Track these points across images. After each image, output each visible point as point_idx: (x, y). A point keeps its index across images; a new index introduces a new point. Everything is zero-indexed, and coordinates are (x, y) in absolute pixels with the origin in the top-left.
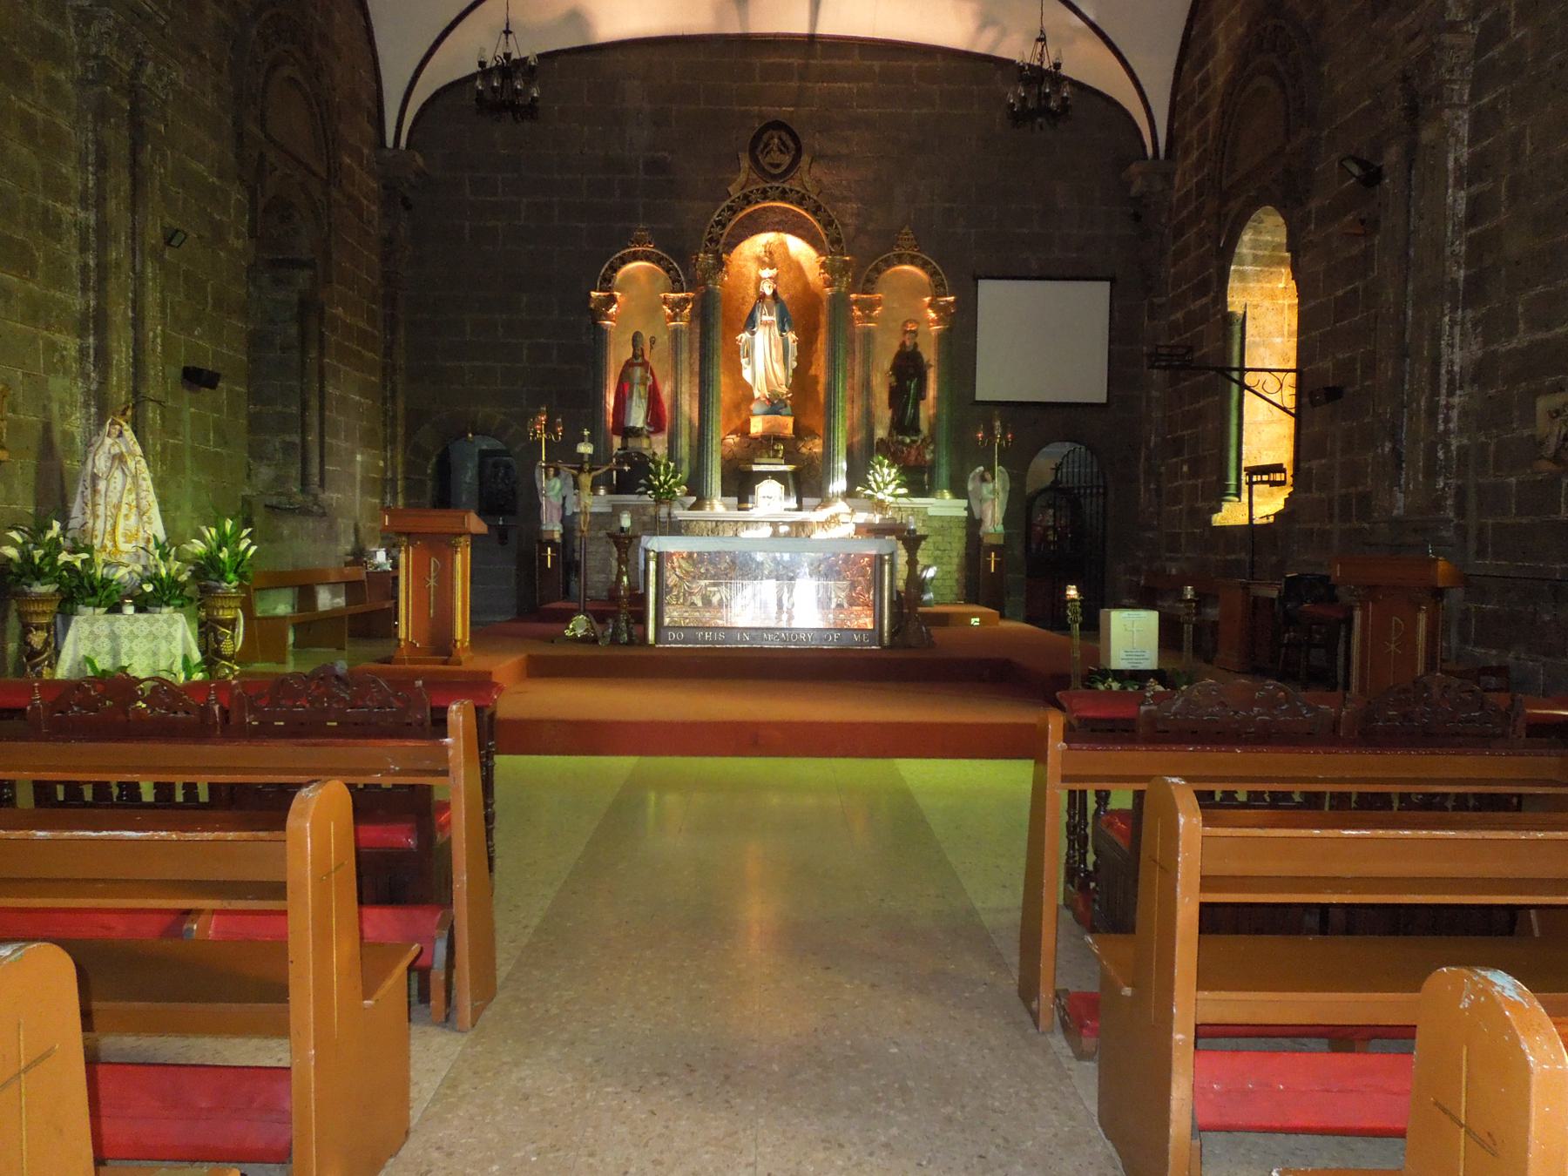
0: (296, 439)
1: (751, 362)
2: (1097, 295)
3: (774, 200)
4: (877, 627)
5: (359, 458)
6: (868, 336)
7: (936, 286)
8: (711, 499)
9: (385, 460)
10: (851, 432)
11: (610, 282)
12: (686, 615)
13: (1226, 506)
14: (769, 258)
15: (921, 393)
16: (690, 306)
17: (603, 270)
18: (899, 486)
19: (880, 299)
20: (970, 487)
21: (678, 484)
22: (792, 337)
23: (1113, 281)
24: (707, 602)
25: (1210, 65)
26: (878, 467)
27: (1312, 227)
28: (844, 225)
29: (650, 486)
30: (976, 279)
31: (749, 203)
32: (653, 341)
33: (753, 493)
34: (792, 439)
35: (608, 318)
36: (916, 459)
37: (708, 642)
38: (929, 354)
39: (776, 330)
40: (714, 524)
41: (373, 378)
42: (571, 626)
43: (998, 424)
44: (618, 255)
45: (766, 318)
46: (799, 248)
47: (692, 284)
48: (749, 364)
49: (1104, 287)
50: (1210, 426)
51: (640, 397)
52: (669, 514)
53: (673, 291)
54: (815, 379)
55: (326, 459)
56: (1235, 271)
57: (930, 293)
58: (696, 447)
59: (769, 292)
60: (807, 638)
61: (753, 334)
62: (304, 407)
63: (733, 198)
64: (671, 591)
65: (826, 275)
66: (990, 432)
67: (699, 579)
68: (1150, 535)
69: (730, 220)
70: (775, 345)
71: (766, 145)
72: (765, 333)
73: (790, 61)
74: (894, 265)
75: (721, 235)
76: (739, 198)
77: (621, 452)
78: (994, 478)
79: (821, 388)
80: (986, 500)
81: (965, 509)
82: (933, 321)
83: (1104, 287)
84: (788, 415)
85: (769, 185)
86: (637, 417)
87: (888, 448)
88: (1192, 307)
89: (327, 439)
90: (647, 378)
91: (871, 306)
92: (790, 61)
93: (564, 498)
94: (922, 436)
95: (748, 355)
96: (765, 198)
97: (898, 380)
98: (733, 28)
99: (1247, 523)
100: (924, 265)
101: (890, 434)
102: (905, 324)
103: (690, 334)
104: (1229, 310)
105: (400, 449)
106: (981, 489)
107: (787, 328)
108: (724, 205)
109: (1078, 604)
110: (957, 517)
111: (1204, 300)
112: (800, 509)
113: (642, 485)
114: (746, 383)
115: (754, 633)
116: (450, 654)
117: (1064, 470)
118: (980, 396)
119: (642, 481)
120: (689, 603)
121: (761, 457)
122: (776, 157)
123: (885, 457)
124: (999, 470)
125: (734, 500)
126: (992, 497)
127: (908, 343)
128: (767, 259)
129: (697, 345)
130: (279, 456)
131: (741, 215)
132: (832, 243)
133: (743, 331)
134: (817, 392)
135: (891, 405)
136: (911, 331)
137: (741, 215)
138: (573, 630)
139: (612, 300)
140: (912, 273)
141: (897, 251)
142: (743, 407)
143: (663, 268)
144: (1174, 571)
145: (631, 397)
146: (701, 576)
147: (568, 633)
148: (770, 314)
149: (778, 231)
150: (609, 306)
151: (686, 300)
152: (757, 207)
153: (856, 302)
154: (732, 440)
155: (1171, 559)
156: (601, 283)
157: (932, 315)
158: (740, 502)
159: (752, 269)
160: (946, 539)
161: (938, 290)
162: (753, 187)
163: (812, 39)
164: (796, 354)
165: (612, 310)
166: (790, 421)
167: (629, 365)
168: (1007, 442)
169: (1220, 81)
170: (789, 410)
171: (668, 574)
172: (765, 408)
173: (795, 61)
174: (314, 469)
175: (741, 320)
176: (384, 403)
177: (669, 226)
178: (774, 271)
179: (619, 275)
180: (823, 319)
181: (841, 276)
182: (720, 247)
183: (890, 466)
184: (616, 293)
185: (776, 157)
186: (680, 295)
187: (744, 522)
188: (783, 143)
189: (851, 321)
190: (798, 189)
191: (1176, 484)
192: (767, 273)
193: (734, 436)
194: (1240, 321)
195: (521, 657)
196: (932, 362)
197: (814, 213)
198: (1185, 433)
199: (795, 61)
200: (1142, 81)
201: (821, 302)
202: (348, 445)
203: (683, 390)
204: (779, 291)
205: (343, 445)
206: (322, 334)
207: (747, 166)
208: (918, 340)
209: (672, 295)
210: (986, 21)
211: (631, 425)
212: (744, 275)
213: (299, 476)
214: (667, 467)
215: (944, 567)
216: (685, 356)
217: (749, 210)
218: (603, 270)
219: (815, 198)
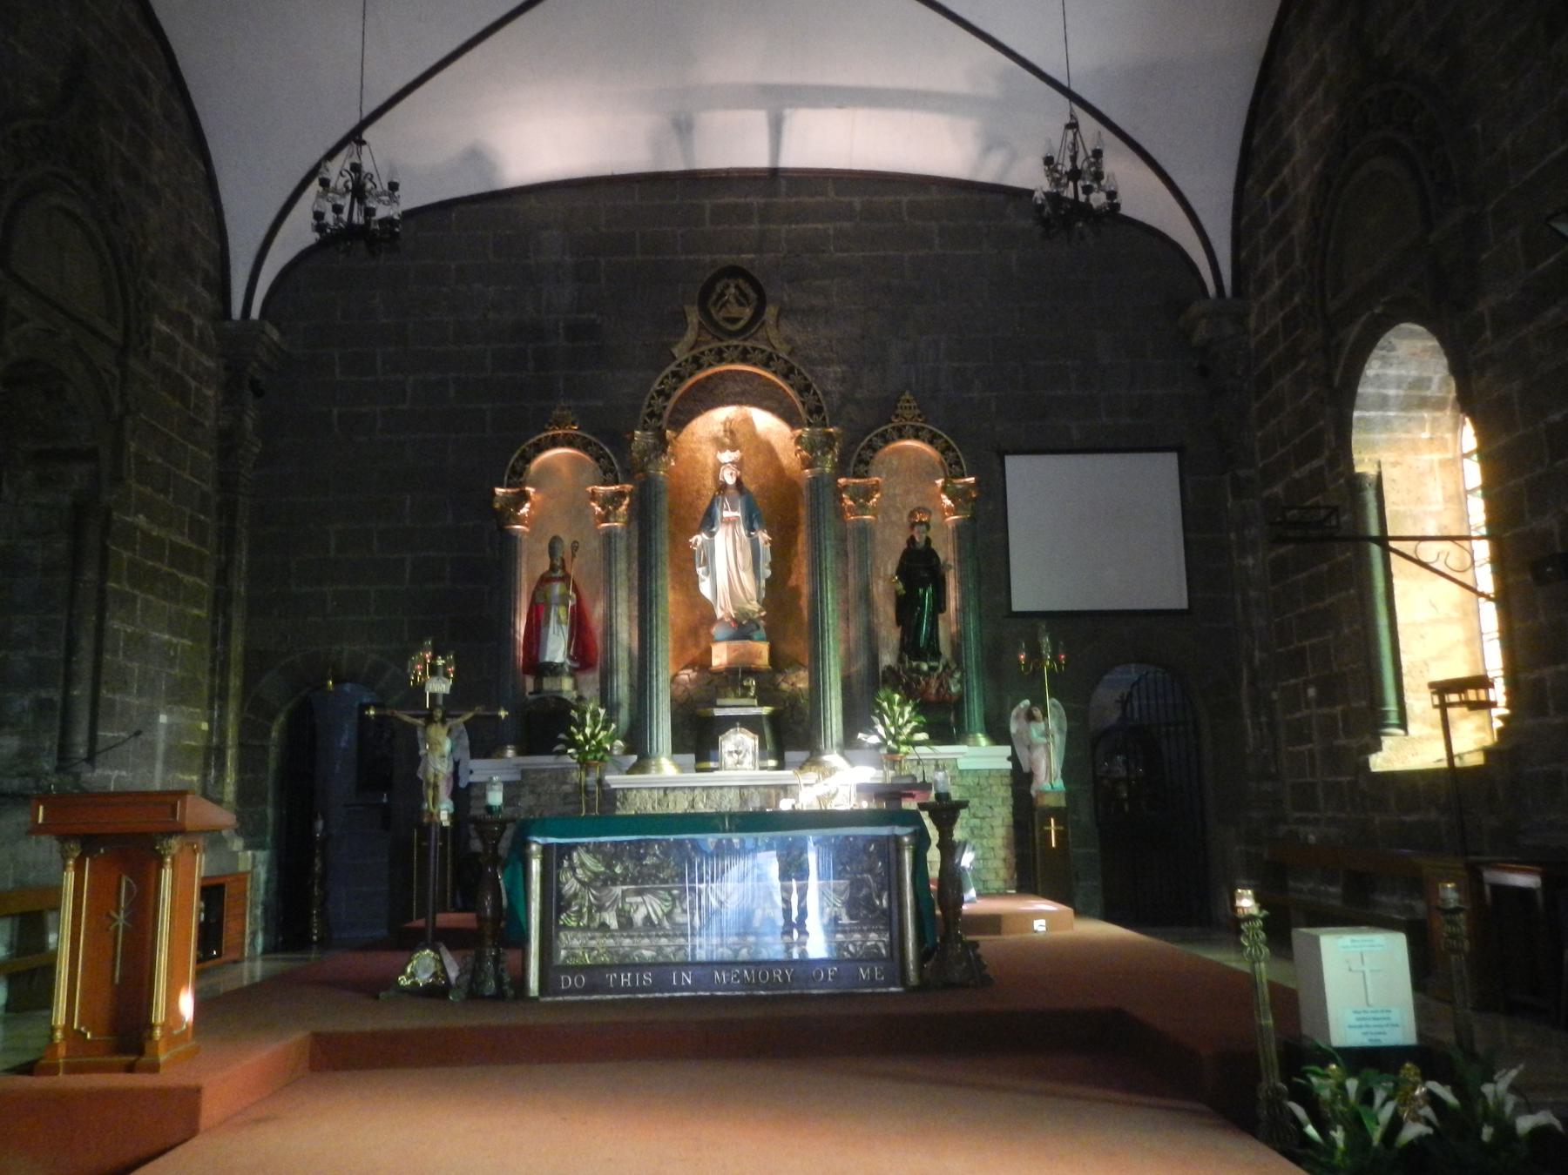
0: (56, 696)
1: (711, 573)
2: (1160, 471)
3: (732, 362)
4: (896, 954)
5: (163, 719)
6: (864, 531)
7: (950, 465)
8: (657, 757)
9: (210, 721)
10: (848, 659)
11: (521, 475)
12: (593, 943)
13: (1387, 742)
14: (732, 437)
15: (939, 604)
16: (627, 501)
17: (512, 461)
18: (916, 730)
20: (1013, 729)
21: (612, 739)
22: (763, 536)
23: (1180, 450)
24: (626, 923)
25: (1286, 171)
26: (885, 704)
27: (1488, 334)
28: (825, 393)
29: (572, 743)
30: (1001, 455)
31: (700, 367)
32: (575, 547)
33: (715, 745)
34: (769, 671)
35: (519, 521)
36: (938, 691)
37: (625, 990)
38: (946, 551)
40: (662, 793)
41: (196, 611)
42: (409, 970)
43: (1046, 640)
44: (531, 441)
45: (726, 514)
46: (766, 422)
47: (629, 476)
48: (707, 573)
49: (1171, 459)
50: (1346, 631)
51: (559, 622)
52: (600, 782)
53: (605, 483)
54: (796, 591)
55: (100, 722)
56: (1360, 419)
57: (942, 474)
58: (636, 685)
59: (731, 481)
60: (784, 974)
61: (712, 535)
62: (71, 648)
63: (677, 362)
64: (569, 906)
65: (804, 453)
66: (1035, 653)
67: (614, 884)
68: (1267, 786)
69: (675, 389)
70: (741, 549)
71: (722, 295)
72: (727, 534)
73: (748, 200)
74: (893, 440)
75: (665, 408)
76: (686, 361)
77: (534, 697)
78: (1045, 715)
79: (804, 602)
80: (1037, 746)
81: (1009, 759)
82: (949, 507)
83: (1171, 459)
84: (761, 640)
85: (725, 344)
86: (557, 649)
87: (899, 678)
88: (1296, 475)
89: (104, 693)
90: (570, 597)
91: (868, 497)
92: (748, 200)
93: (456, 764)
94: (942, 661)
95: (705, 562)
96: (721, 360)
97: (906, 587)
98: (675, 164)
99: (1444, 764)
101: (900, 660)
102: (912, 514)
103: (628, 539)
104: (1358, 469)
105: (233, 706)
106: (1028, 732)
107: (756, 525)
108: (667, 371)
109: (1259, 923)
110: (998, 770)
111: (1315, 463)
112: (781, 767)
113: (562, 741)
114: (706, 600)
115: (700, 971)
116: (140, 1051)
117: (1136, 703)
118: (1022, 601)
119: (562, 736)
120: (596, 924)
121: (726, 696)
122: (734, 310)
123: (895, 690)
124: (1054, 705)
125: (690, 758)
126: (1044, 740)
127: (917, 539)
128: (727, 441)
129: (635, 553)
130: (28, 719)
131: (690, 382)
132: (810, 413)
133: (698, 532)
134: (800, 609)
135: (900, 620)
136: (921, 523)
137: (690, 382)
138: (413, 975)
139: (524, 497)
140: (916, 450)
141: (896, 422)
142: (702, 632)
143: (591, 455)
144: (1312, 838)
145: (547, 623)
146: (613, 880)
147: (404, 981)
148: (734, 509)
149: (740, 403)
150: (519, 506)
151: (621, 495)
152: (710, 371)
153: (845, 487)
154: (687, 675)
155: (1303, 821)
156: (509, 478)
157: (947, 502)
158: (698, 760)
159: (708, 454)
160: (985, 802)
161: (953, 469)
162: (705, 348)
163: (774, 173)
164: (769, 558)
165: (524, 510)
166: (763, 648)
167: (545, 580)
168: (1059, 665)
169: (1302, 187)
170: (762, 632)
171: (563, 879)
172: (730, 632)
173: (756, 201)
174: (80, 737)
175: (695, 519)
176: (214, 642)
177: (600, 403)
178: (736, 455)
179: (534, 466)
180: (803, 512)
181: (824, 454)
182: (664, 423)
183: (902, 704)
184: (527, 488)
185: (734, 310)
186: (613, 488)
187: (704, 788)
188: (745, 296)
189: (840, 513)
190: (763, 347)
191: (1298, 715)
192: (727, 457)
193: (689, 671)
194: (1374, 484)
195: (297, 1037)
196: (951, 562)
197: (786, 377)
198: (1306, 643)
199: (756, 201)
200: (1195, 206)
201: (800, 491)
202: (144, 700)
203: (619, 611)
204: (745, 479)
205: (134, 701)
206: (105, 548)
207: (695, 320)
208: (931, 534)
209: (602, 488)
210: (991, 143)
211: (547, 659)
212: (697, 462)
213: (55, 748)
214: (595, 715)
215: (985, 842)
216: (621, 566)
217: (701, 375)
218: (512, 461)
219: (786, 357)
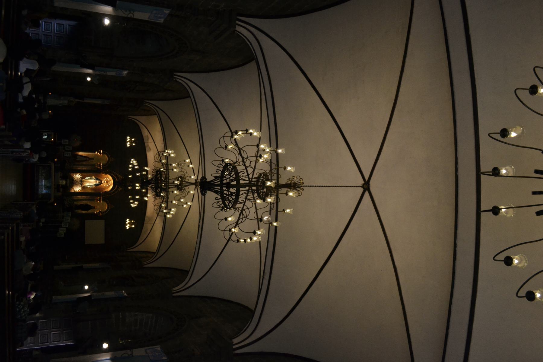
1: (89, 179)
19: (101, 202)
22: (94, 186)
35: (97, 153)
38: (90, 211)
39: (95, 183)
46: (111, 187)
59: (102, 182)
61: (95, 179)
91: (100, 201)
100: (107, 210)
131: (115, 177)
133: (95, 178)
137: (115, 177)
139: (100, 153)
141: (110, 205)
151: (100, 167)
164: (91, 187)
165: (99, 154)
179: (105, 155)
